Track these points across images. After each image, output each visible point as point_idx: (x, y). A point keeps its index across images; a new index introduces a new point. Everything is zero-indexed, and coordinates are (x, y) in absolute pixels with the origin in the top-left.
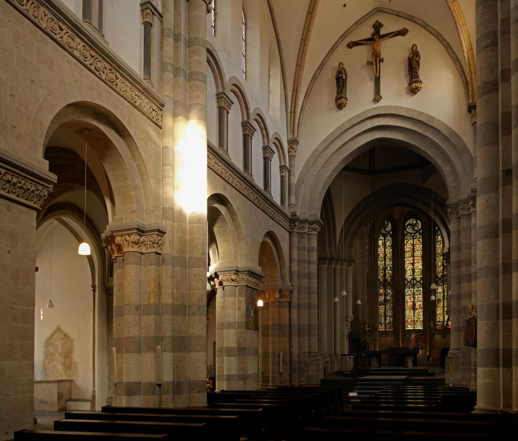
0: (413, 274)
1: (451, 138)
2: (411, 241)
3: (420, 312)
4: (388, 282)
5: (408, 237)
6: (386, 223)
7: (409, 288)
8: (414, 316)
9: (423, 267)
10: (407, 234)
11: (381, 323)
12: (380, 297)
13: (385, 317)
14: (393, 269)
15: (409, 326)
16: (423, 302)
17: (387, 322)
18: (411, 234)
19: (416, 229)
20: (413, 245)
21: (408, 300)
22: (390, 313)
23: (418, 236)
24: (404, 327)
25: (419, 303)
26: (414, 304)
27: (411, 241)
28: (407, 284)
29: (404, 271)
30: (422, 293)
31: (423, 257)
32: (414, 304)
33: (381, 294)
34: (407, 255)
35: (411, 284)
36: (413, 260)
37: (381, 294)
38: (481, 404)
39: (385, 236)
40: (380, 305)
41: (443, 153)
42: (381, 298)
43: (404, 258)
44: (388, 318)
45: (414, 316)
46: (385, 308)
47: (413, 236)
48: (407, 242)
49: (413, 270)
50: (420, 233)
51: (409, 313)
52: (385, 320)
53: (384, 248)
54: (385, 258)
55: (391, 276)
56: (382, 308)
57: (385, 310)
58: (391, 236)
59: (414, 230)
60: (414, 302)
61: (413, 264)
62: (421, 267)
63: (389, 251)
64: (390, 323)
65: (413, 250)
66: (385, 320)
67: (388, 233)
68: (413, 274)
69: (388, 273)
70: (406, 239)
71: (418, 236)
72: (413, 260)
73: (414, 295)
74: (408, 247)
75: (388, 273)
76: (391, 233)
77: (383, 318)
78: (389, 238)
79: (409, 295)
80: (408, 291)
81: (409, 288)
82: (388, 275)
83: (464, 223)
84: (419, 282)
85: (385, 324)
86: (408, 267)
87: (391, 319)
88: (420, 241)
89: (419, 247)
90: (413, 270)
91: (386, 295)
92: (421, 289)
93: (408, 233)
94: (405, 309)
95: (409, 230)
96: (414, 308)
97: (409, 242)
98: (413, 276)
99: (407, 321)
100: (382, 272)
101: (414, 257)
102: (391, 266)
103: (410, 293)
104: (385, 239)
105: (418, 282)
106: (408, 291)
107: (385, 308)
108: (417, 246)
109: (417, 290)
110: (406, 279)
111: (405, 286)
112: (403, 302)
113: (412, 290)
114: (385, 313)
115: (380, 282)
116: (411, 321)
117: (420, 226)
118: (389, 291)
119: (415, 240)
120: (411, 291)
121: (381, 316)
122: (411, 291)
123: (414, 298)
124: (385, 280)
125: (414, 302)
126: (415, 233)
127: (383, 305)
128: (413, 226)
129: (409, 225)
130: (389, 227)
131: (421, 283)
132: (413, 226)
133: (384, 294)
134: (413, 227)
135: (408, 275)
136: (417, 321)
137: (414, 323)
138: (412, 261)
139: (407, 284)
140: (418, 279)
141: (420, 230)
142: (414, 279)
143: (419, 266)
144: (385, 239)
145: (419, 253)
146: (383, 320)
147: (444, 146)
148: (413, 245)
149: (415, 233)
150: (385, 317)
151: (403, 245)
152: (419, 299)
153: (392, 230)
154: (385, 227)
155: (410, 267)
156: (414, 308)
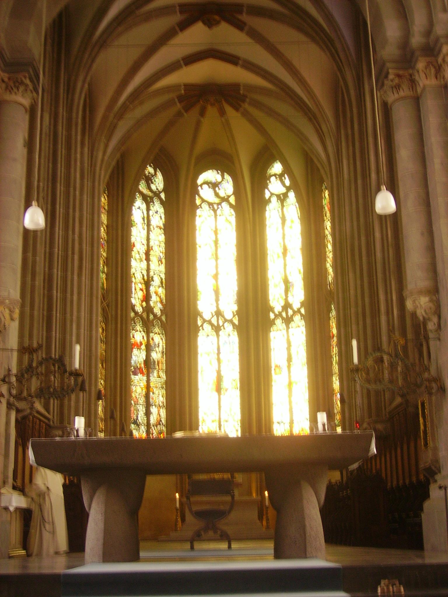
4: (155, 316)
6: (150, 170)
11: (135, 422)
12: (135, 351)
13: (148, 405)
17: (153, 419)
18: (210, 204)
22: (159, 397)
33: (139, 346)
37: (139, 346)
39: (148, 201)
40: (135, 374)
42: (138, 357)
44: (154, 410)
46: (148, 381)
47: (215, 211)
52: (148, 413)
53: (146, 225)
54: (147, 254)
55: (161, 302)
56: (138, 384)
57: (148, 387)
58: (162, 202)
59: (217, 195)
63: (158, 238)
64: (159, 422)
66: (148, 413)
67: (157, 194)
69: (156, 293)
75: (156, 293)
76: (163, 196)
77: (142, 410)
78: (157, 207)
82: (154, 298)
84: (231, 321)
85: (148, 425)
87: (163, 413)
91: (149, 349)
95: (206, 193)
100: (142, 290)
102: (163, 276)
104: (148, 209)
107: (148, 381)
114: (147, 396)
115: (136, 313)
121: (137, 403)
124: (149, 309)
126: (219, 204)
127: (142, 373)
128: (214, 185)
130: (159, 183)
131: (234, 325)
132: (214, 185)
133: (146, 345)
135: (205, 305)
144: (148, 209)
149: (219, 204)
150: (148, 405)
153: (165, 190)
154: (149, 180)
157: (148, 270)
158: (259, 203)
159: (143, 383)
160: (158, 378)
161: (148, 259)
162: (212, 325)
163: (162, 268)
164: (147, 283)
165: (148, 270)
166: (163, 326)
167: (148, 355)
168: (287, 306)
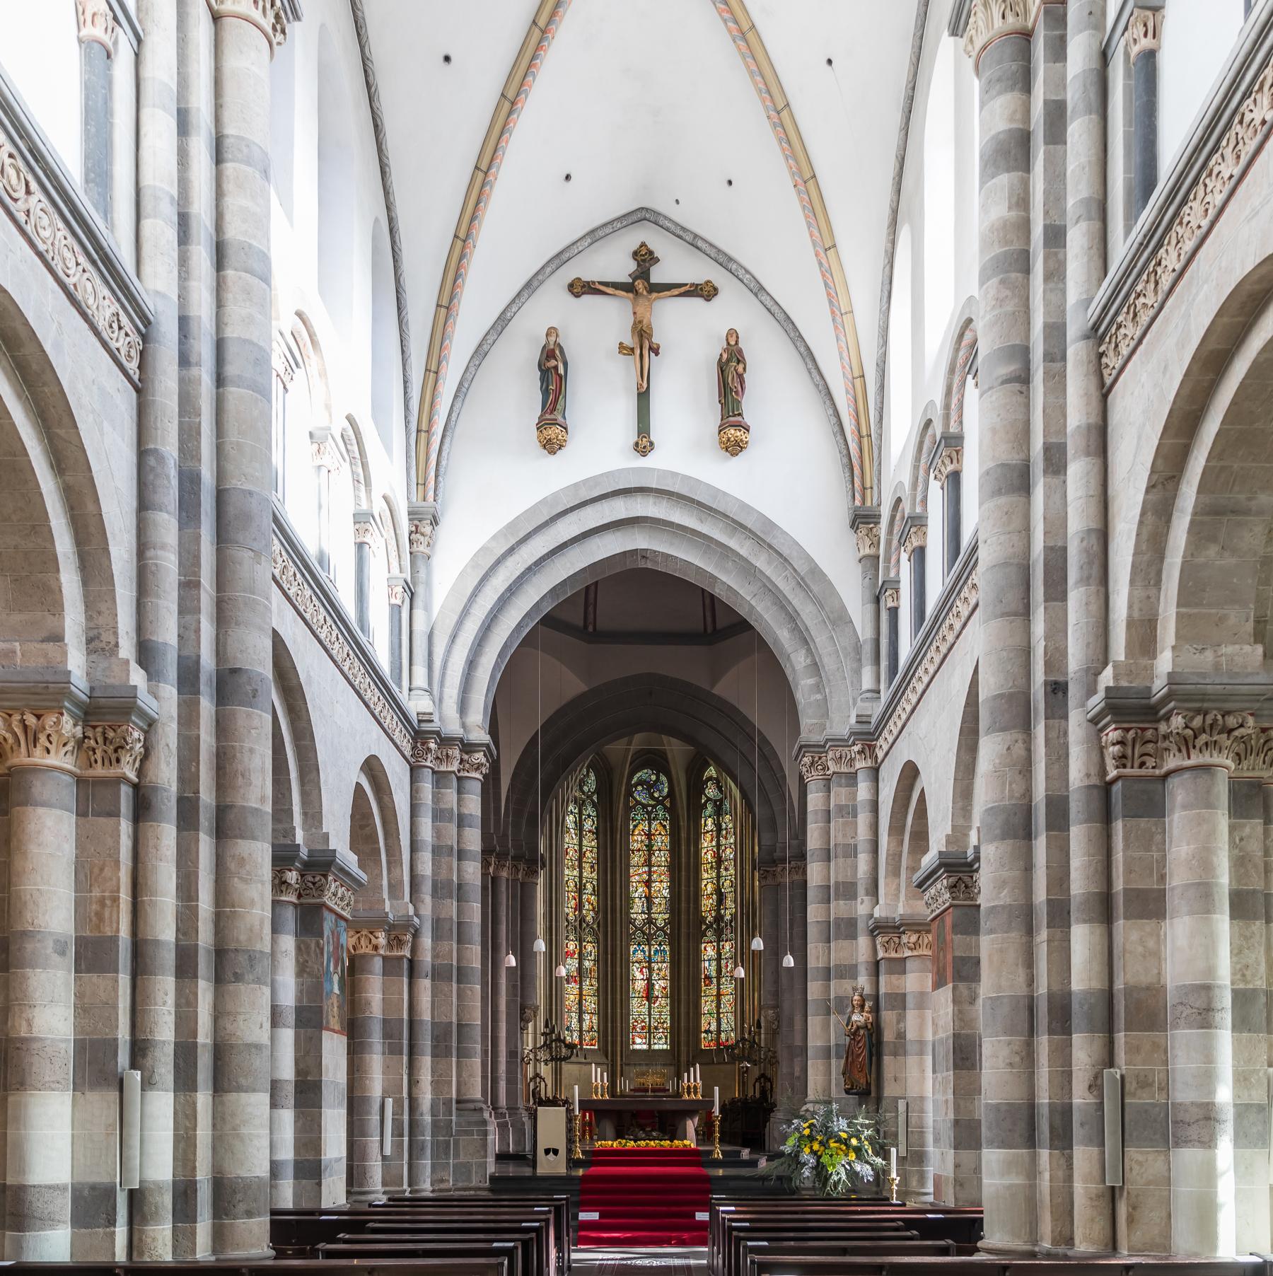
0: (649, 908)
1: (812, 580)
2: (644, 826)
3: (662, 1009)
5: (638, 814)
7: (639, 945)
8: (650, 1015)
9: (670, 893)
10: (634, 807)
14: (600, 891)
15: (638, 1040)
16: (672, 980)
18: (645, 806)
19: (656, 795)
20: (649, 835)
21: (638, 975)
22: (591, 1004)
23: (661, 813)
24: (626, 1042)
25: (660, 985)
26: (650, 986)
27: (644, 826)
28: (634, 933)
29: (629, 900)
30: (668, 959)
31: (674, 868)
32: (650, 986)
34: (636, 859)
35: (643, 933)
36: (650, 873)
38: (998, 1237)
41: (792, 618)
43: (628, 866)
44: (586, 1017)
45: (650, 1015)
46: (581, 989)
47: (649, 813)
48: (635, 826)
49: (649, 899)
50: (665, 807)
51: (637, 1007)
52: (581, 1020)
57: (581, 995)
59: (652, 797)
60: (649, 979)
61: (648, 884)
62: (666, 893)
65: (650, 847)
66: (581, 1020)
68: (649, 908)
70: (634, 820)
71: (661, 813)
72: (650, 873)
73: (650, 962)
74: (637, 840)
79: (639, 963)
80: (636, 950)
81: (639, 945)
83: (839, 795)
84: (662, 929)
85: (581, 1031)
86: (638, 891)
88: (664, 827)
89: (662, 841)
90: (649, 899)
92: (667, 948)
93: (638, 803)
94: (628, 998)
95: (640, 796)
96: (649, 996)
97: (641, 827)
98: (649, 914)
99: (634, 1028)
101: (650, 866)
103: (640, 955)
105: (659, 929)
106: (637, 953)
107: (581, 989)
108: (659, 838)
109: (656, 951)
110: (631, 922)
111: (629, 938)
112: (627, 979)
113: (646, 948)
116: (643, 1028)
117: (666, 790)
118: (589, 947)
119: (655, 824)
120: (643, 951)
121: (570, 1011)
122: (643, 951)
123: (650, 969)
125: (649, 979)
126: (654, 806)
128: (649, 786)
129: (640, 783)
134: (648, 789)
135: (637, 911)
136: (656, 1028)
137: (650, 1032)
138: (645, 877)
139: (634, 933)
140: (660, 923)
141: (665, 798)
142: (650, 921)
143: (662, 888)
145: (661, 858)
146: (575, 1021)
147: (797, 600)
148: (649, 835)
149: (654, 806)
151: (627, 834)
152: (662, 973)
155: (642, 889)
156: (649, 996)
157: (581, 877)
158: (696, 810)
159: (576, 991)
160: (590, 986)
161: (580, 867)
162: (643, 933)
163: (594, 875)
164: (580, 889)
165: (581, 877)
166: (595, 934)
167: (580, 963)
168: (719, 918)
